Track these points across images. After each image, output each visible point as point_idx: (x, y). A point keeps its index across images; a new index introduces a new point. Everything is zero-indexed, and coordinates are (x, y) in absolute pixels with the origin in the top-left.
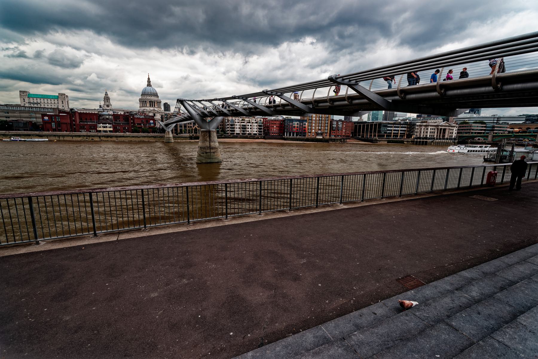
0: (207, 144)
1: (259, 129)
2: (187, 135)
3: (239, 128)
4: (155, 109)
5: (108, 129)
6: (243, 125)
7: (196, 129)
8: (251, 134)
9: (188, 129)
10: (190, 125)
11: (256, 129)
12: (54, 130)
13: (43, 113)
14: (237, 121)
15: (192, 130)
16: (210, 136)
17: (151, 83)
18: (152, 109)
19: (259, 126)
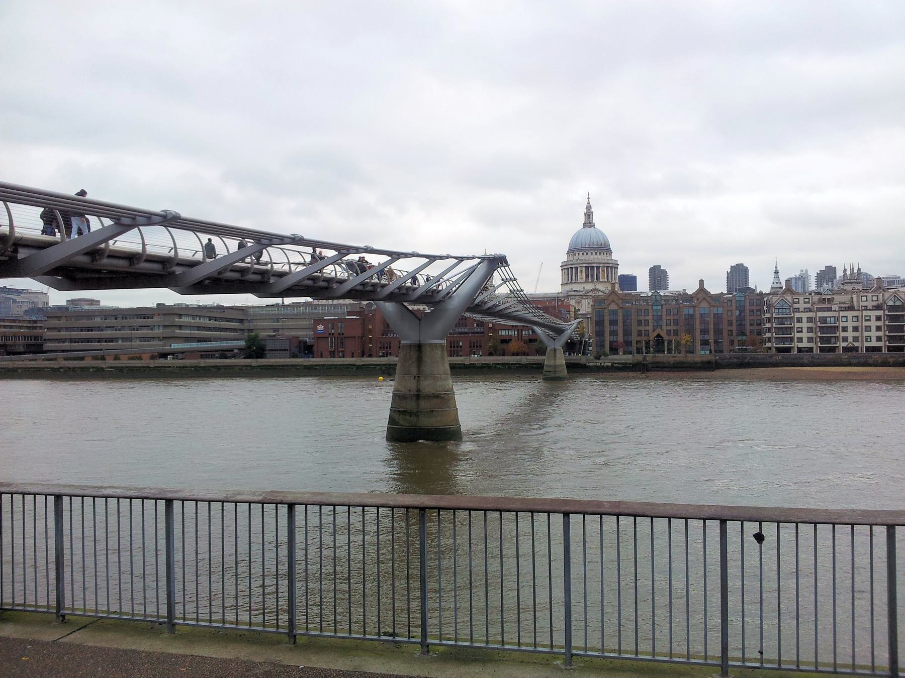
0: (412, 384)
1: (891, 328)
2: (628, 359)
3: (810, 330)
4: (600, 287)
6: (824, 320)
7: (659, 340)
8: (856, 349)
9: (634, 338)
11: (878, 329)
12: (332, 354)
13: (317, 317)
14: (802, 306)
15: (647, 343)
16: (420, 361)
17: (596, 219)
18: (590, 287)
19: (892, 318)
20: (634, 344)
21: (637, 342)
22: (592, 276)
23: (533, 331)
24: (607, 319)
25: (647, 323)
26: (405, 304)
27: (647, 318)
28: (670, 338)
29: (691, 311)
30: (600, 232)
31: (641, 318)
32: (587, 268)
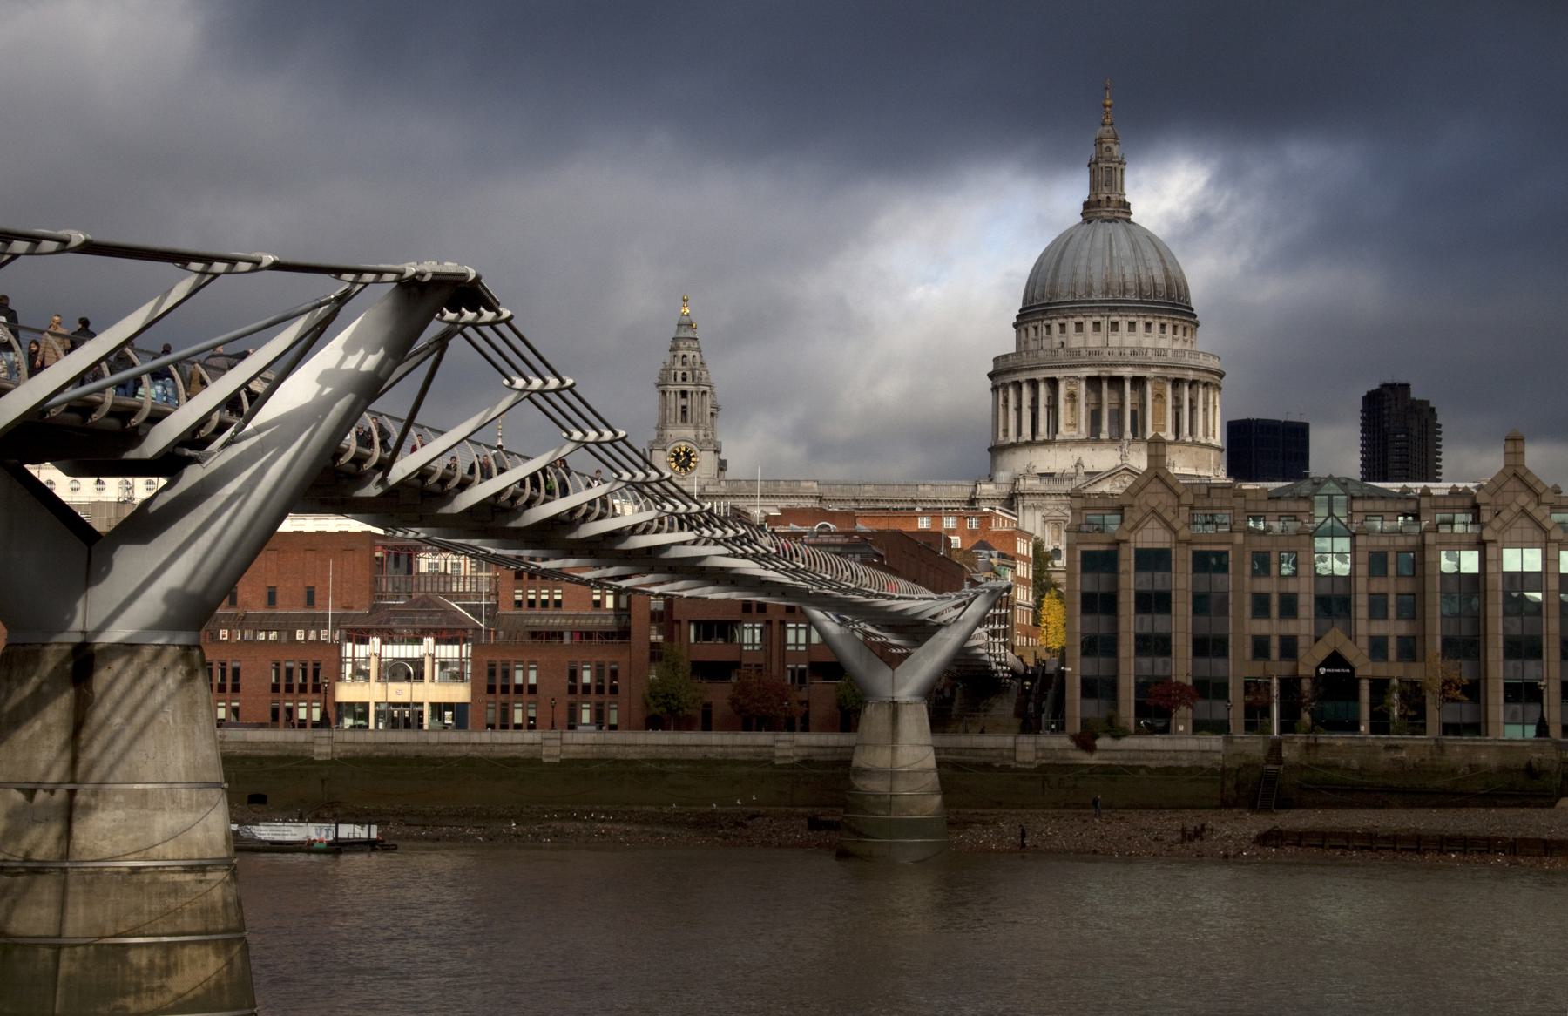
5: (428, 692)
9: (1237, 667)
10: (1272, 627)
15: (1290, 685)
18: (1102, 459)
20: (1236, 693)
21: (1250, 686)
22: (1117, 416)
23: (811, 622)
24: (1130, 582)
25: (1289, 606)
26: (47, 473)
27: (1291, 587)
28: (1382, 670)
29: (1470, 562)
30: (1151, 238)
31: (1263, 585)
32: (1093, 382)
